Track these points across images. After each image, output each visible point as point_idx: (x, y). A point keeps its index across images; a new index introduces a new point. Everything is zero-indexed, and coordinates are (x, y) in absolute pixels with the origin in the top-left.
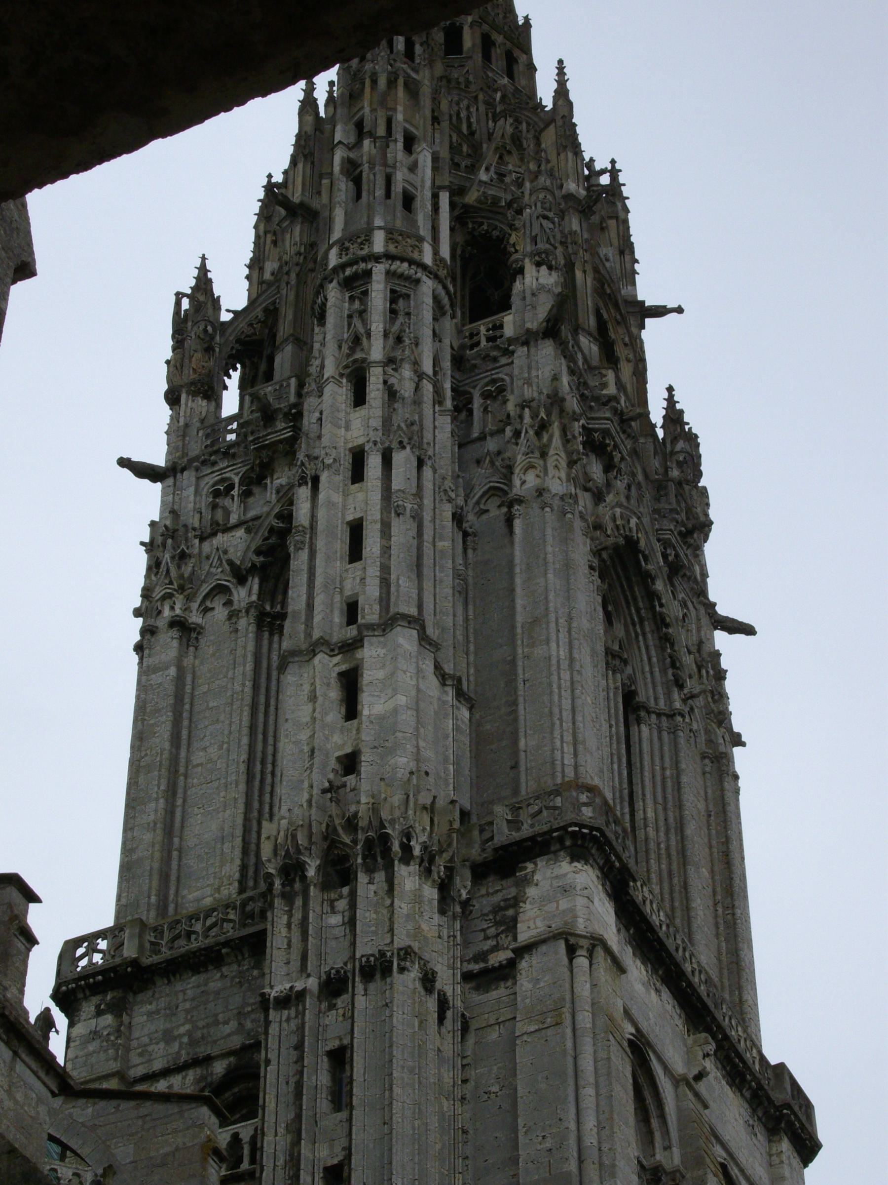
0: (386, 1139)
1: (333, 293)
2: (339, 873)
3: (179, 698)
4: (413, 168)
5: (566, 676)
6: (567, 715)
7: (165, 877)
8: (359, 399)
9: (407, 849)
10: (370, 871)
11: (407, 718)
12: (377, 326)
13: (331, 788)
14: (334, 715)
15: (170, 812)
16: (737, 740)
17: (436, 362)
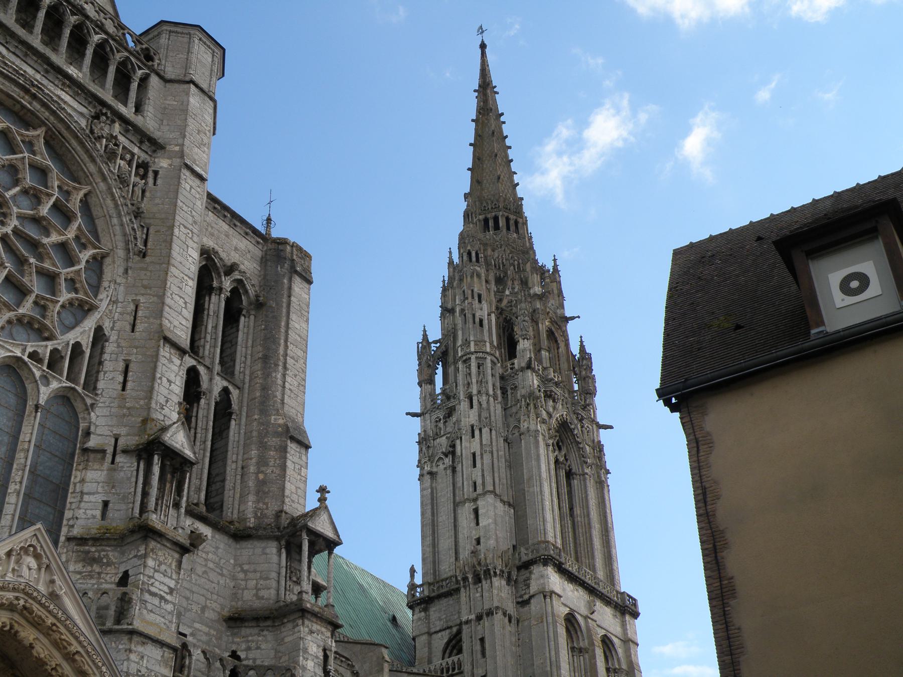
0: (496, 668)
1: (460, 365)
2: (478, 580)
3: (432, 499)
4: (481, 309)
5: (540, 497)
6: (541, 512)
7: (434, 562)
8: (472, 407)
9: (495, 573)
10: (486, 579)
11: (492, 526)
12: (474, 380)
13: (472, 552)
14: (473, 524)
15: (434, 540)
16: (608, 472)
17: (494, 385)
